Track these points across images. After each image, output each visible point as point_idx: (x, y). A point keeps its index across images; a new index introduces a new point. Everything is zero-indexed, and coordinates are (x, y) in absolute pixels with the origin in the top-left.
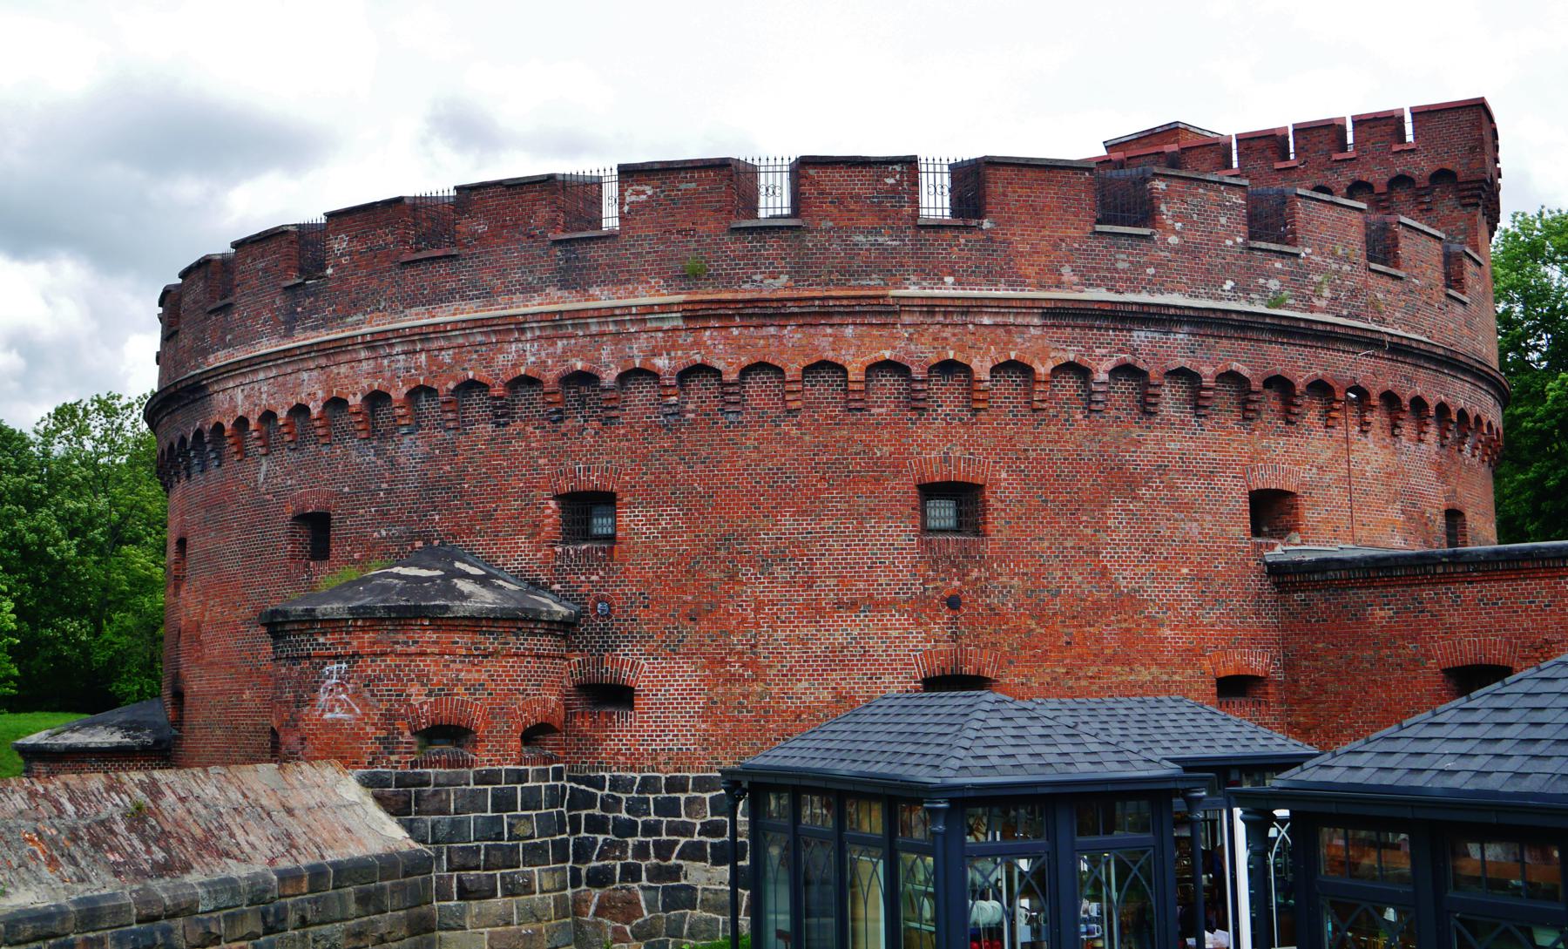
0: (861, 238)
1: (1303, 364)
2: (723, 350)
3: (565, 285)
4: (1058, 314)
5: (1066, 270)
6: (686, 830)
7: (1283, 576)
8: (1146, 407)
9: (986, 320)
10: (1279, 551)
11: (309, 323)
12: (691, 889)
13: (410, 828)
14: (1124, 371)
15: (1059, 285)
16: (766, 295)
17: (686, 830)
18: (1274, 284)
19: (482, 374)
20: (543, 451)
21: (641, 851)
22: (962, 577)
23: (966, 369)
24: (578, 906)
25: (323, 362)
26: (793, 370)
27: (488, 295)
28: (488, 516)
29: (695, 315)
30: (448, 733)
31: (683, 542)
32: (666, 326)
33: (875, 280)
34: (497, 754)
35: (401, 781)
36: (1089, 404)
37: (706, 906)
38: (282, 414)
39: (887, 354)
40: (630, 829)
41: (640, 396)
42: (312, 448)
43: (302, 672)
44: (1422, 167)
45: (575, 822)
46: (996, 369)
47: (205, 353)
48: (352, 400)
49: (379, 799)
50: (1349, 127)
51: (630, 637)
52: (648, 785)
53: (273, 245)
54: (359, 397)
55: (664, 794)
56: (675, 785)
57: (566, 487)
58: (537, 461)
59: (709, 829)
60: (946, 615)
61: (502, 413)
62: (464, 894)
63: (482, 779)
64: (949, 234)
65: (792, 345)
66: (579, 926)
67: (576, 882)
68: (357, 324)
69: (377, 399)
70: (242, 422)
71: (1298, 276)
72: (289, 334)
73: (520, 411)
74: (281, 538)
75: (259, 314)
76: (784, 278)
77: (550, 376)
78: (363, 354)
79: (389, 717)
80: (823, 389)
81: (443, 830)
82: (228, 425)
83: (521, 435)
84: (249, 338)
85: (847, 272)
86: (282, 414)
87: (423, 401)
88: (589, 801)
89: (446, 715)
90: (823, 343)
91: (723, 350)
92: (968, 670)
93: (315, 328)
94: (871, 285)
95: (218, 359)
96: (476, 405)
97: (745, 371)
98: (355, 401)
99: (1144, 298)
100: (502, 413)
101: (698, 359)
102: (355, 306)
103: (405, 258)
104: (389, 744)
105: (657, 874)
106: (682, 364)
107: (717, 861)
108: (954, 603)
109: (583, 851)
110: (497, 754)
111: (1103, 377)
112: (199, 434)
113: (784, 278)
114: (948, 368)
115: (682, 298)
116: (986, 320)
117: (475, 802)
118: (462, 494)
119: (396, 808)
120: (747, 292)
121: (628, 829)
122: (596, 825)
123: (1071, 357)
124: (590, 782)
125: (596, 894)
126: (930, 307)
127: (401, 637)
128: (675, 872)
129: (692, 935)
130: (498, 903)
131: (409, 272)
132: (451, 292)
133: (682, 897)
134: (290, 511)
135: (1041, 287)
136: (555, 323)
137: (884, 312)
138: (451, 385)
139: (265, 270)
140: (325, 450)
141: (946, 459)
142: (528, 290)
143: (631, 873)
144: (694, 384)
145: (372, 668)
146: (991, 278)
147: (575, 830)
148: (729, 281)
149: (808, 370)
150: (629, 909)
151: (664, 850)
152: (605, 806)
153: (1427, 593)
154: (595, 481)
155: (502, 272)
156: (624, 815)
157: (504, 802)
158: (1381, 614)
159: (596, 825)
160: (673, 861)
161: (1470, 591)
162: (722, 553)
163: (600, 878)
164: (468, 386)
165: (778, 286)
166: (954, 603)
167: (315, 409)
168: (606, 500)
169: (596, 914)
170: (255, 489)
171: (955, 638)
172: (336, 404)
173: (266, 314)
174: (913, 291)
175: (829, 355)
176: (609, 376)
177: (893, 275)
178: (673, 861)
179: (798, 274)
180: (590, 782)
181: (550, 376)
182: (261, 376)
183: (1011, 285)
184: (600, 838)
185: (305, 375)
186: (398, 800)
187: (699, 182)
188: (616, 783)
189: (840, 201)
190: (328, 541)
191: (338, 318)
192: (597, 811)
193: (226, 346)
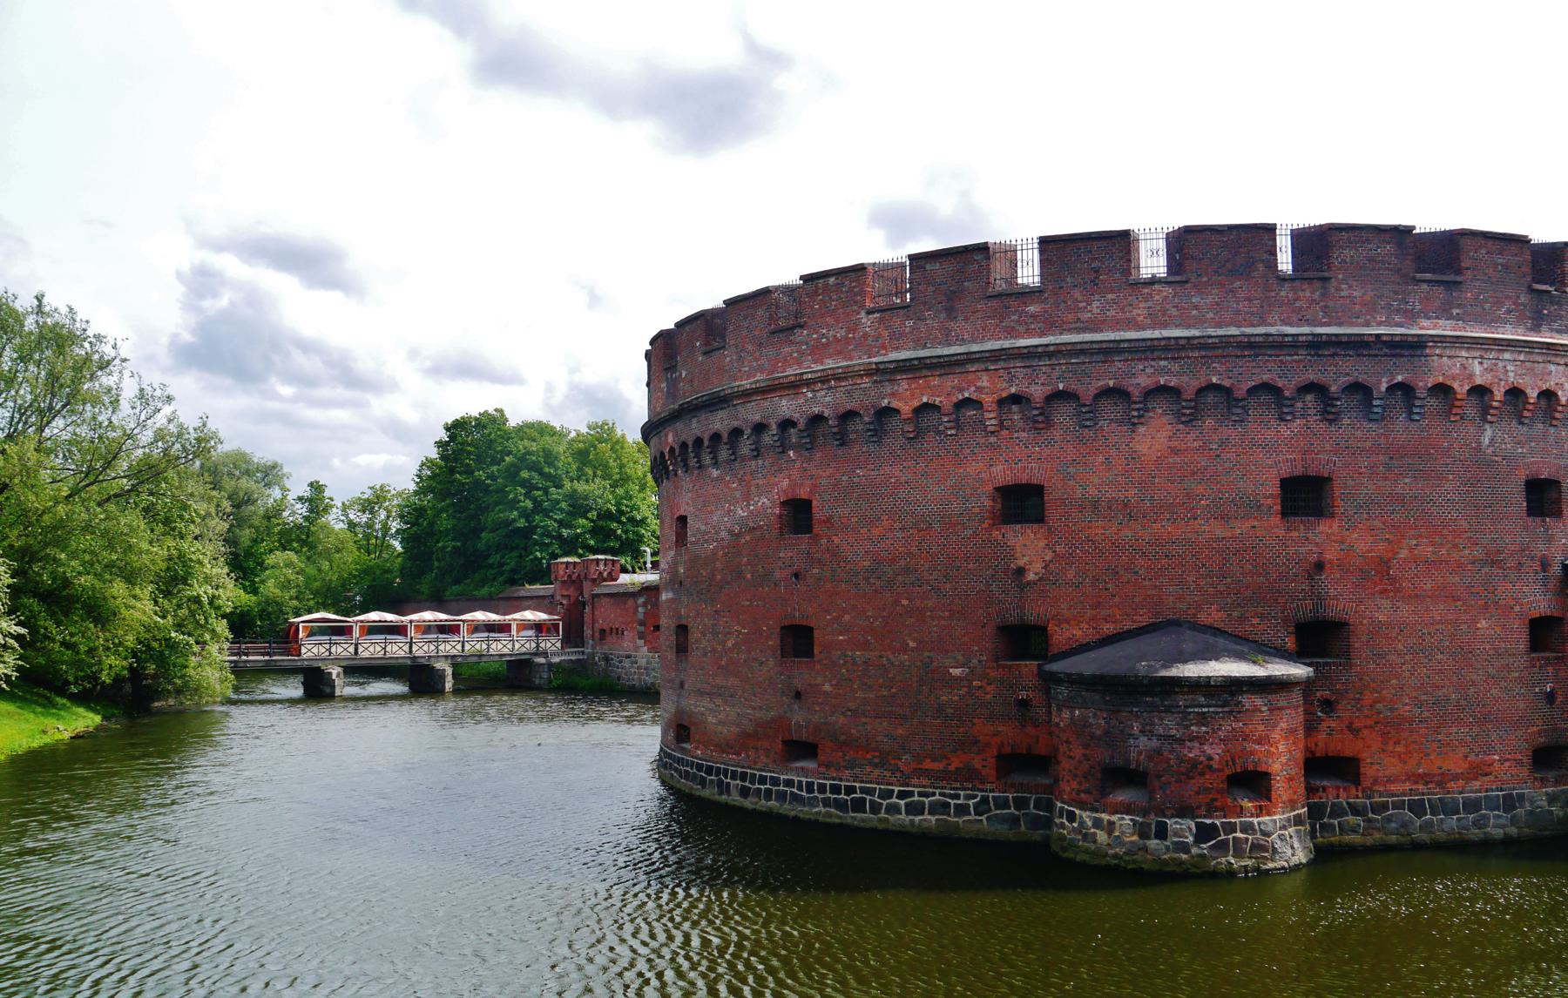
38: (1533, 394)
42: (1540, 426)
47: (1411, 317)
53: (1513, 248)
70: (1480, 391)
72: (1536, 328)
75: (1498, 303)
82: (1461, 388)
93: (1559, 332)
95: (1444, 328)
134: (1523, 476)
139: (1506, 267)
140: (1552, 430)
170: (1479, 448)
173: (1508, 305)
182: (1507, 356)
185: (1553, 367)
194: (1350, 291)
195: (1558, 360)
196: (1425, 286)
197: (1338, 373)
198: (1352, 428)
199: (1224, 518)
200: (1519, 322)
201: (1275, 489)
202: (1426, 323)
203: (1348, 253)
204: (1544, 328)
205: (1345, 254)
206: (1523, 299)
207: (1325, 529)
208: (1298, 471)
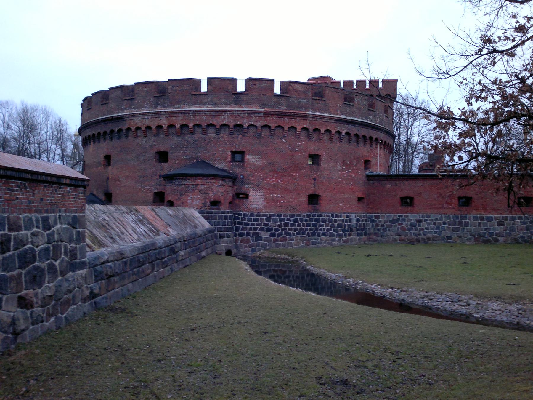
0: (300, 100)
1: (374, 134)
2: (272, 122)
3: (236, 104)
4: (338, 120)
5: (339, 111)
6: (260, 225)
7: (369, 177)
8: (349, 141)
9: (324, 120)
10: (368, 173)
11: (163, 106)
12: (261, 237)
13: (209, 222)
14: (347, 133)
15: (337, 114)
16: (281, 111)
17: (260, 225)
18: (371, 117)
19: (215, 123)
20: (228, 141)
21: (251, 229)
22: (316, 174)
23: (296, 129)
24: (236, 241)
25: (168, 116)
26: (286, 128)
27: (216, 104)
28: (214, 155)
29: (266, 114)
30: (215, 203)
31: (261, 163)
32: (260, 115)
33: (303, 110)
34: (224, 207)
35: (208, 213)
36: (340, 140)
37: (265, 241)
38: (154, 128)
39: (305, 126)
40: (248, 224)
41: (252, 130)
42: (162, 136)
43: (182, 188)
44: (383, 93)
45: (235, 223)
46: (325, 131)
47: (123, 110)
48: (176, 125)
49: (203, 216)
50: (368, 82)
51: (248, 183)
52: (252, 215)
53: (150, 85)
54: (179, 125)
55: (255, 217)
56: (258, 215)
57: (234, 150)
58: (226, 143)
59: (265, 225)
60: (313, 182)
61: (218, 132)
62: (221, 237)
63: (223, 212)
64: (318, 101)
65: (286, 123)
66: (236, 245)
67: (235, 235)
68: (178, 108)
69: (183, 126)
70: (138, 128)
71: (375, 116)
72: (156, 107)
73: (222, 131)
74: (152, 158)
75: (145, 102)
76: (285, 108)
77: (231, 125)
78: (180, 115)
79: (205, 199)
80: (291, 132)
81: (216, 223)
83: (222, 137)
84: (140, 107)
85: (299, 108)
86: (154, 128)
87: (196, 128)
88: (238, 218)
89: (217, 199)
90: (293, 122)
91: (272, 122)
92: (317, 193)
94: (302, 111)
96: (211, 130)
97: (276, 127)
98: (178, 126)
99: (351, 118)
100: (218, 132)
101: (266, 123)
102: (177, 103)
103: (193, 93)
104: (204, 204)
105: (253, 234)
106: (262, 125)
107: (267, 231)
108: (315, 179)
109: (237, 229)
110: (224, 207)
111: (344, 134)
112: (120, 130)
113: (285, 108)
114: (316, 130)
115: (263, 110)
116: (324, 120)
117: (221, 217)
118: (207, 149)
119: (207, 219)
120: (277, 110)
121: (248, 224)
122: (240, 224)
123: (338, 130)
124: (238, 214)
125: (240, 238)
126: (314, 117)
127: (208, 181)
128: (258, 234)
129: (261, 247)
130: (226, 239)
131: (194, 97)
132: (206, 102)
133: (259, 239)
135: (334, 114)
136: (232, 113)
137: (304, 117)
138: (206, 124)
139: (147, 91)
141: (314, 149)
142: (226, 104)
143: (248, 234)
144: (264, 129)
145: (200, 187)
146: (325, 111)
147: (235, 225)
148: (274, 107)
149: (289, 128)
150: (248, 241)
151: (255, 229)
152: (242, 220)
153: (398, 182)
154: (240, 149)
155: (220, 99)
156: (246, 222)
157: (226, 218)
158: (388, 186)
159: (240, 224)
160: (258, 231)
161: (406, 182)
162: (269, 166)
163: (241, 235)
164: (209, 125)
165: (284, 109)
166: (315, 179)
167: (165, 127)
168: (242, 153)
169: (241, 242)
170: (141, 145)
171: (315, 187)
172: (171, 126)
173: (147, 102)
174: (311, 113)
175: (294, 125)
176: (245, 126)
177: (307, 109)
178: (258, 231)
179: (288, 106)
180: (238, 214)
181: (231, 125)
182: (146, 117)
183: (329, 113)
184: (241, 226)
186: (208, 216)
187: (267, 83)
188: (244, 215)
189: (297, 91)
190: (167, 158)
191: (172, 105)
192: (240, 221)
193: (131, 108)
194: (112, 105)
195: (163, 116)
196: (126, 101)
197: (108, 127)
198: (116, 142)
199: (97, 167)
200: (150, 106)
201: (103, 159)
202: (125, 111)
203: (112, 95)
204: (159, 107)
205: (112, 96)
206: (152, 99)
207: (110, 168)
208: (106, 154)
